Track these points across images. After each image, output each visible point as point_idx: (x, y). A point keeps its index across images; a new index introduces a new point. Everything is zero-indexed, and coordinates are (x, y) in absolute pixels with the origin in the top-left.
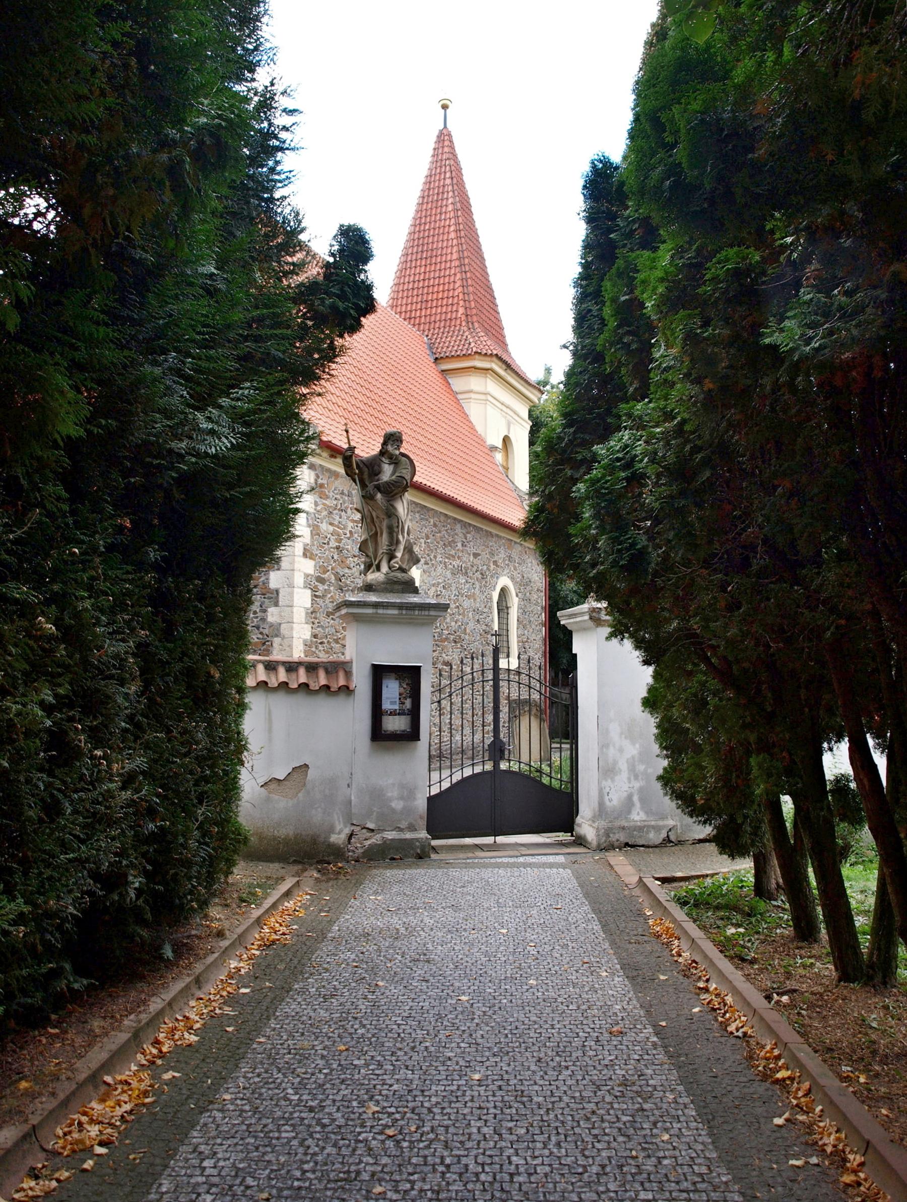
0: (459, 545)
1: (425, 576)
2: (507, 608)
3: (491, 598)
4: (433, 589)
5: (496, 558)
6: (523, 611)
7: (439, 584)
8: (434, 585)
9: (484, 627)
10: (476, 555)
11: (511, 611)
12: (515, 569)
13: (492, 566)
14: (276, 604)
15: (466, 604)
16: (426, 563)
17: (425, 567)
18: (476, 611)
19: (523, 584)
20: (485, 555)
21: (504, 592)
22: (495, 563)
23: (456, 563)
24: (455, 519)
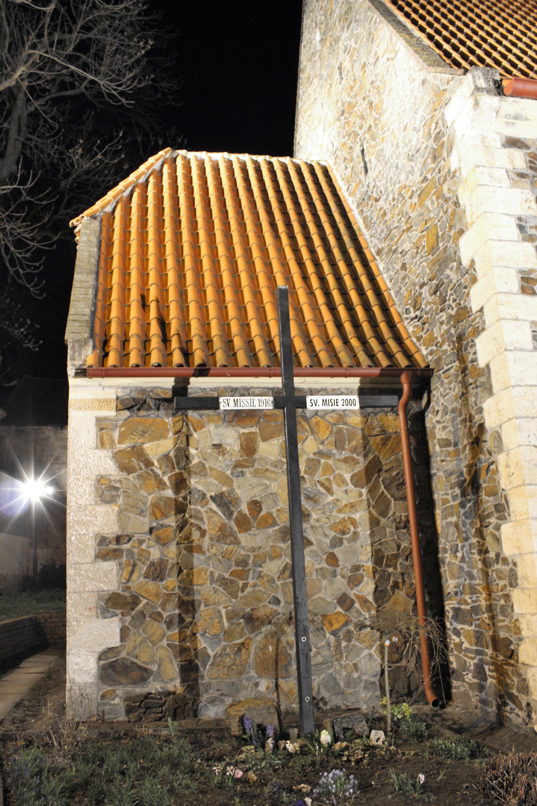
14: (490, 391)
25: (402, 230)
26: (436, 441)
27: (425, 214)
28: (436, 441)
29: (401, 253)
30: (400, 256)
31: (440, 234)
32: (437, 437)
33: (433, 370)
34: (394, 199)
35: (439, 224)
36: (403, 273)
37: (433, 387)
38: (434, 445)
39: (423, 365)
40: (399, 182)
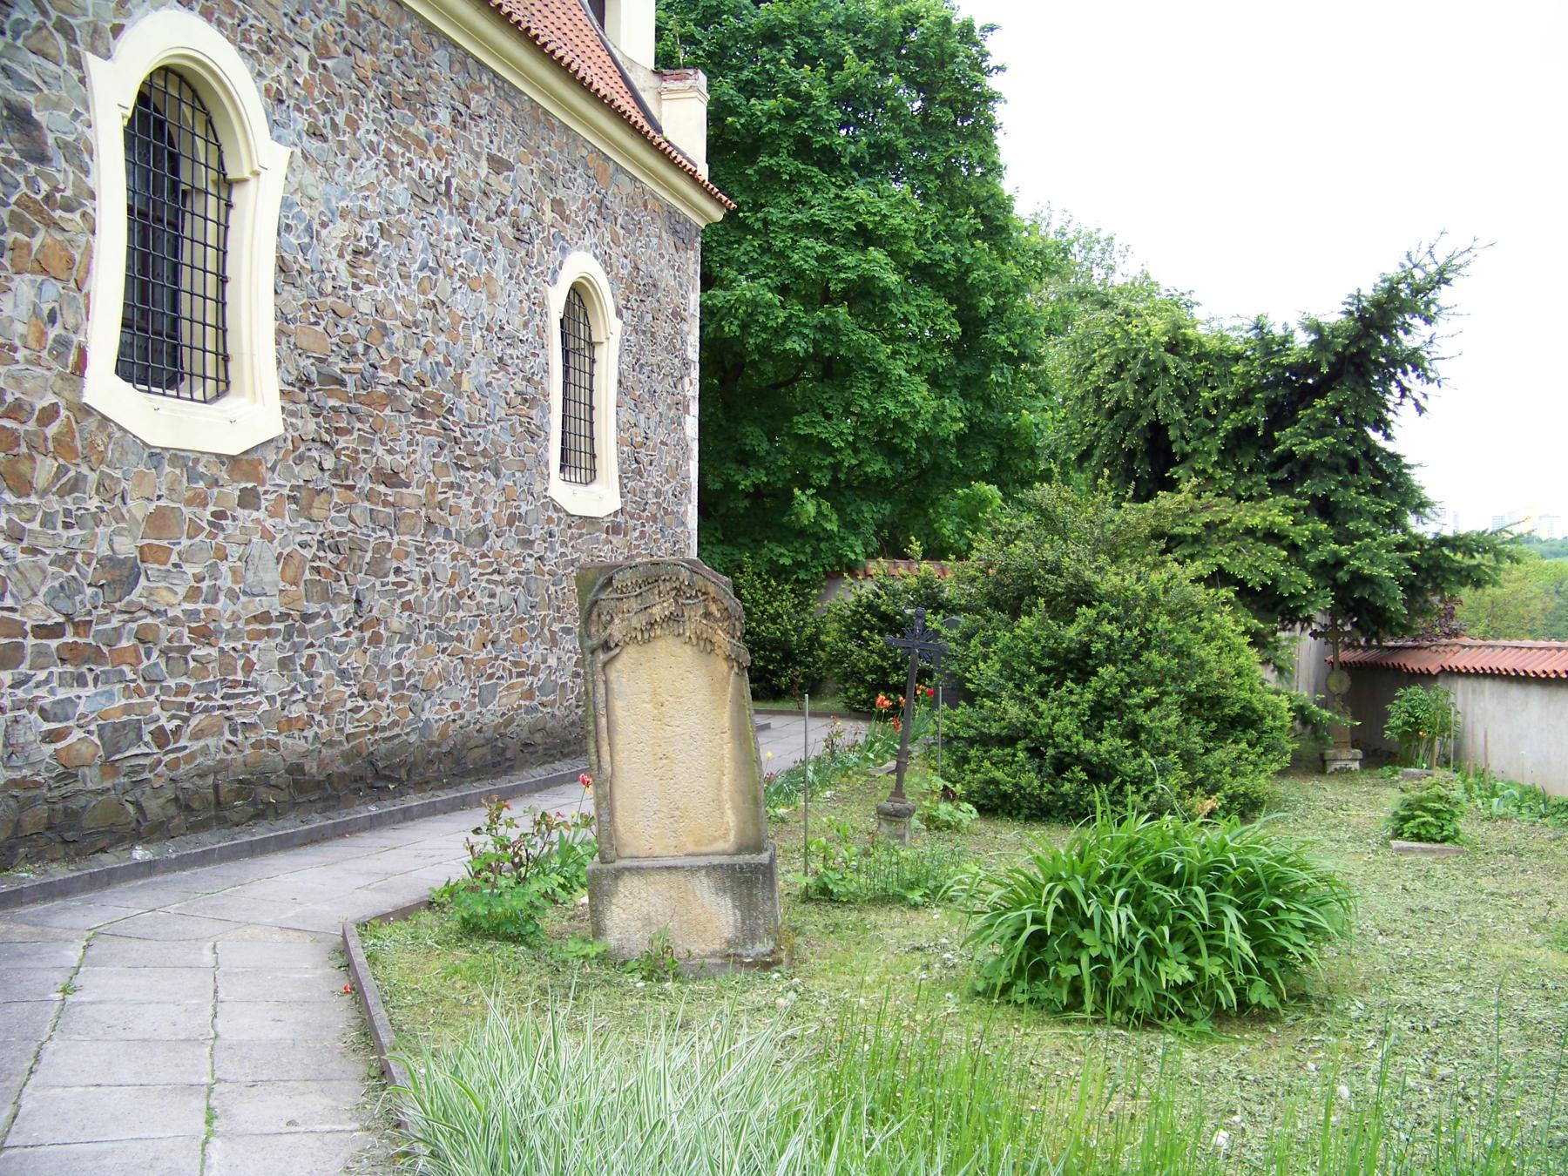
0: (444, 116)
1: (310, 177)
2: (592, 345)
3: (542, 305)
4: (340, 229)
5: (560, 193)
6: (635, 362)
7: (363, 216)
8: (344, 214)
9: (520, 385)
10: (498, 165)
11: (600, 354)
12: (615, 241)
13: (549, 216)
15: (462, 302)
16: (315, 133)
17: (313, 145)
18: (494, 330)
19: (638, 289)
20: (526, 175)
21: (579, 295)
22: (557, 205)
23: (432, 167)
24: (431, 29)
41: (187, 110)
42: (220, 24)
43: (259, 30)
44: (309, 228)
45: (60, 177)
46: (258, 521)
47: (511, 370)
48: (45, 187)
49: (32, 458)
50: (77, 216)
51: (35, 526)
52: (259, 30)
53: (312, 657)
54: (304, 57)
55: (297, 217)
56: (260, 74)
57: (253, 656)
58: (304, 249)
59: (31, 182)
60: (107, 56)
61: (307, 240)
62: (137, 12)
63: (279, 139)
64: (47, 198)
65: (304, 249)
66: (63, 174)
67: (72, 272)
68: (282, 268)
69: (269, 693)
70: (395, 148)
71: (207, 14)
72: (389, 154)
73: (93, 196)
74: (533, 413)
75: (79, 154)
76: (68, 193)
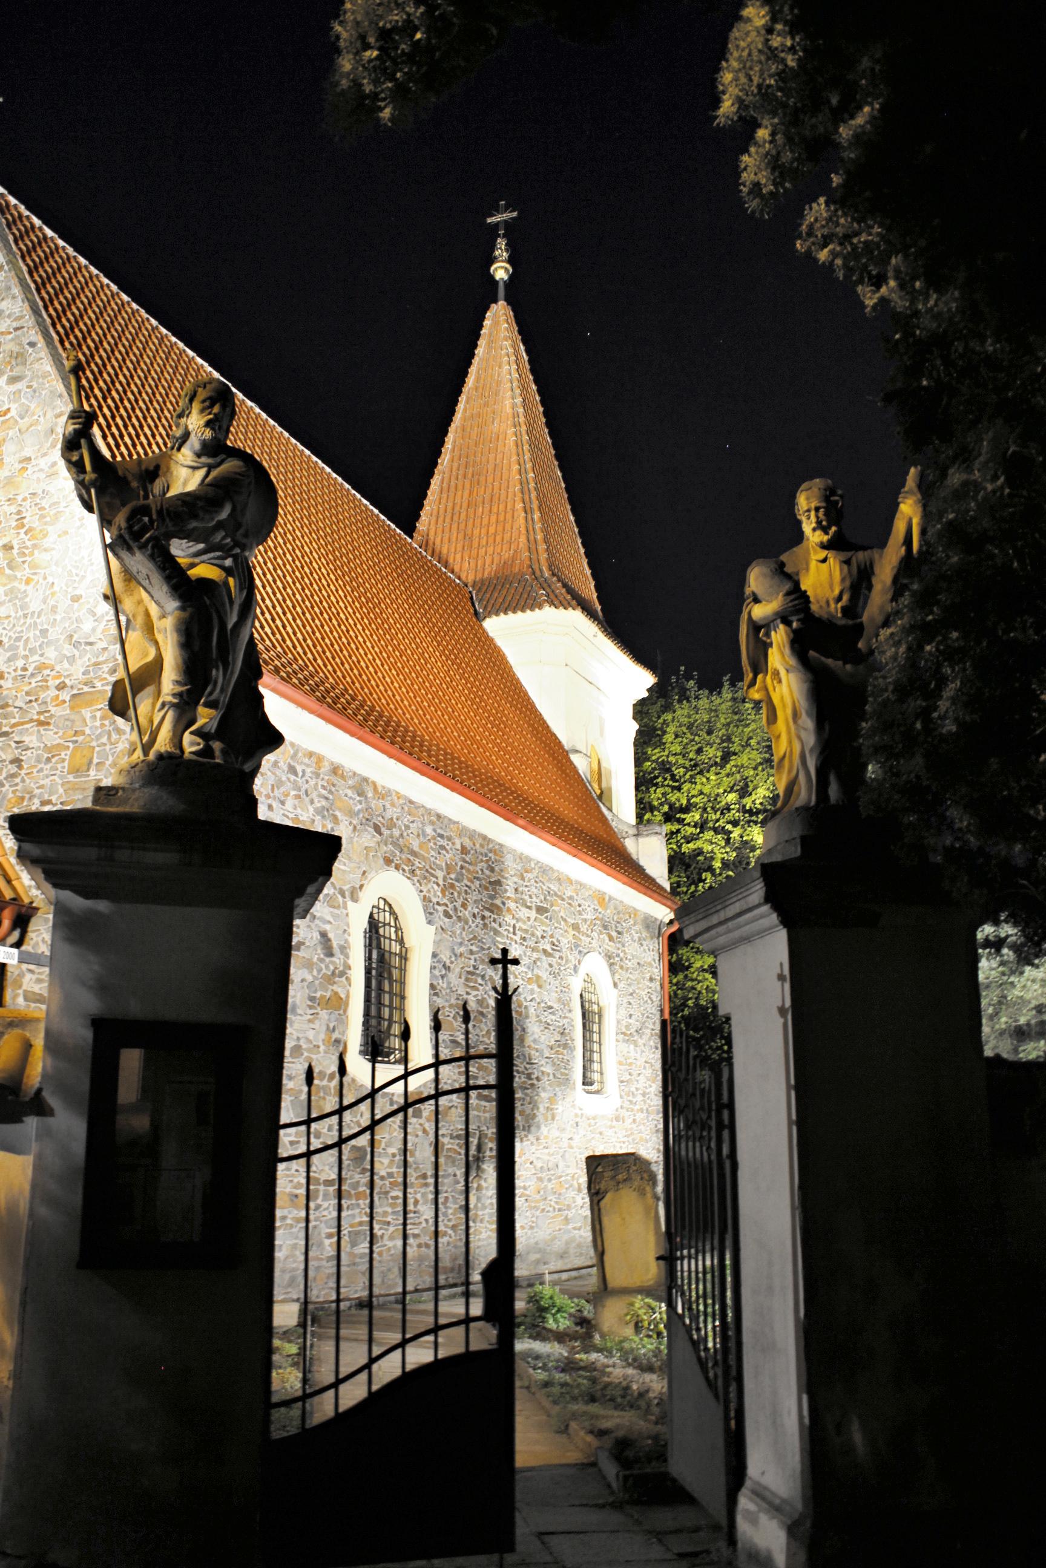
25: (29, 716)
26: (21, 991)
27: (78, 723)
28: (21, 991)
29: (17, 742)
30: (14, 745)
31: (95, 761)
32: (24, 987)
33: (37, 909)
34: (25, 669)
35: (97, 749)
36: (13, 769)
37: (32, 927)
38: (16, 996)
39: (26, 901)
40: (42, 655)
41: (387, 914)
42: (404, 870)
43: (420, 869)
44: (444, 966)
45: (338, 961)
46: (421, 1125)
47: (552, 1028)
48: (332, 968)
49: (324, 1098)
50: (343, 979)
51: (325, 1131)
52: (420, 869)
53: (447, 1198)
54: (440, 874)
55: (439, 961)
56: (421, 891)
57: (419, 1196)
58: (442, 977)
59: (327, 967)
60: (356, 901)
61: (444, 972)
62: (369, 876)
63: (429, 922)
64: (333, 973)
65: (442, 977)
66: (338, 959)
67: (338, 1004)
68: (432, 987)
69: (425, 1217)
70: (487, 914)
71: (397, 868)
72: (483, 918)
73: (350, 968)
74: (565, 1052)
75: (344, 949)
76: (341, 969)
